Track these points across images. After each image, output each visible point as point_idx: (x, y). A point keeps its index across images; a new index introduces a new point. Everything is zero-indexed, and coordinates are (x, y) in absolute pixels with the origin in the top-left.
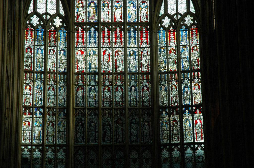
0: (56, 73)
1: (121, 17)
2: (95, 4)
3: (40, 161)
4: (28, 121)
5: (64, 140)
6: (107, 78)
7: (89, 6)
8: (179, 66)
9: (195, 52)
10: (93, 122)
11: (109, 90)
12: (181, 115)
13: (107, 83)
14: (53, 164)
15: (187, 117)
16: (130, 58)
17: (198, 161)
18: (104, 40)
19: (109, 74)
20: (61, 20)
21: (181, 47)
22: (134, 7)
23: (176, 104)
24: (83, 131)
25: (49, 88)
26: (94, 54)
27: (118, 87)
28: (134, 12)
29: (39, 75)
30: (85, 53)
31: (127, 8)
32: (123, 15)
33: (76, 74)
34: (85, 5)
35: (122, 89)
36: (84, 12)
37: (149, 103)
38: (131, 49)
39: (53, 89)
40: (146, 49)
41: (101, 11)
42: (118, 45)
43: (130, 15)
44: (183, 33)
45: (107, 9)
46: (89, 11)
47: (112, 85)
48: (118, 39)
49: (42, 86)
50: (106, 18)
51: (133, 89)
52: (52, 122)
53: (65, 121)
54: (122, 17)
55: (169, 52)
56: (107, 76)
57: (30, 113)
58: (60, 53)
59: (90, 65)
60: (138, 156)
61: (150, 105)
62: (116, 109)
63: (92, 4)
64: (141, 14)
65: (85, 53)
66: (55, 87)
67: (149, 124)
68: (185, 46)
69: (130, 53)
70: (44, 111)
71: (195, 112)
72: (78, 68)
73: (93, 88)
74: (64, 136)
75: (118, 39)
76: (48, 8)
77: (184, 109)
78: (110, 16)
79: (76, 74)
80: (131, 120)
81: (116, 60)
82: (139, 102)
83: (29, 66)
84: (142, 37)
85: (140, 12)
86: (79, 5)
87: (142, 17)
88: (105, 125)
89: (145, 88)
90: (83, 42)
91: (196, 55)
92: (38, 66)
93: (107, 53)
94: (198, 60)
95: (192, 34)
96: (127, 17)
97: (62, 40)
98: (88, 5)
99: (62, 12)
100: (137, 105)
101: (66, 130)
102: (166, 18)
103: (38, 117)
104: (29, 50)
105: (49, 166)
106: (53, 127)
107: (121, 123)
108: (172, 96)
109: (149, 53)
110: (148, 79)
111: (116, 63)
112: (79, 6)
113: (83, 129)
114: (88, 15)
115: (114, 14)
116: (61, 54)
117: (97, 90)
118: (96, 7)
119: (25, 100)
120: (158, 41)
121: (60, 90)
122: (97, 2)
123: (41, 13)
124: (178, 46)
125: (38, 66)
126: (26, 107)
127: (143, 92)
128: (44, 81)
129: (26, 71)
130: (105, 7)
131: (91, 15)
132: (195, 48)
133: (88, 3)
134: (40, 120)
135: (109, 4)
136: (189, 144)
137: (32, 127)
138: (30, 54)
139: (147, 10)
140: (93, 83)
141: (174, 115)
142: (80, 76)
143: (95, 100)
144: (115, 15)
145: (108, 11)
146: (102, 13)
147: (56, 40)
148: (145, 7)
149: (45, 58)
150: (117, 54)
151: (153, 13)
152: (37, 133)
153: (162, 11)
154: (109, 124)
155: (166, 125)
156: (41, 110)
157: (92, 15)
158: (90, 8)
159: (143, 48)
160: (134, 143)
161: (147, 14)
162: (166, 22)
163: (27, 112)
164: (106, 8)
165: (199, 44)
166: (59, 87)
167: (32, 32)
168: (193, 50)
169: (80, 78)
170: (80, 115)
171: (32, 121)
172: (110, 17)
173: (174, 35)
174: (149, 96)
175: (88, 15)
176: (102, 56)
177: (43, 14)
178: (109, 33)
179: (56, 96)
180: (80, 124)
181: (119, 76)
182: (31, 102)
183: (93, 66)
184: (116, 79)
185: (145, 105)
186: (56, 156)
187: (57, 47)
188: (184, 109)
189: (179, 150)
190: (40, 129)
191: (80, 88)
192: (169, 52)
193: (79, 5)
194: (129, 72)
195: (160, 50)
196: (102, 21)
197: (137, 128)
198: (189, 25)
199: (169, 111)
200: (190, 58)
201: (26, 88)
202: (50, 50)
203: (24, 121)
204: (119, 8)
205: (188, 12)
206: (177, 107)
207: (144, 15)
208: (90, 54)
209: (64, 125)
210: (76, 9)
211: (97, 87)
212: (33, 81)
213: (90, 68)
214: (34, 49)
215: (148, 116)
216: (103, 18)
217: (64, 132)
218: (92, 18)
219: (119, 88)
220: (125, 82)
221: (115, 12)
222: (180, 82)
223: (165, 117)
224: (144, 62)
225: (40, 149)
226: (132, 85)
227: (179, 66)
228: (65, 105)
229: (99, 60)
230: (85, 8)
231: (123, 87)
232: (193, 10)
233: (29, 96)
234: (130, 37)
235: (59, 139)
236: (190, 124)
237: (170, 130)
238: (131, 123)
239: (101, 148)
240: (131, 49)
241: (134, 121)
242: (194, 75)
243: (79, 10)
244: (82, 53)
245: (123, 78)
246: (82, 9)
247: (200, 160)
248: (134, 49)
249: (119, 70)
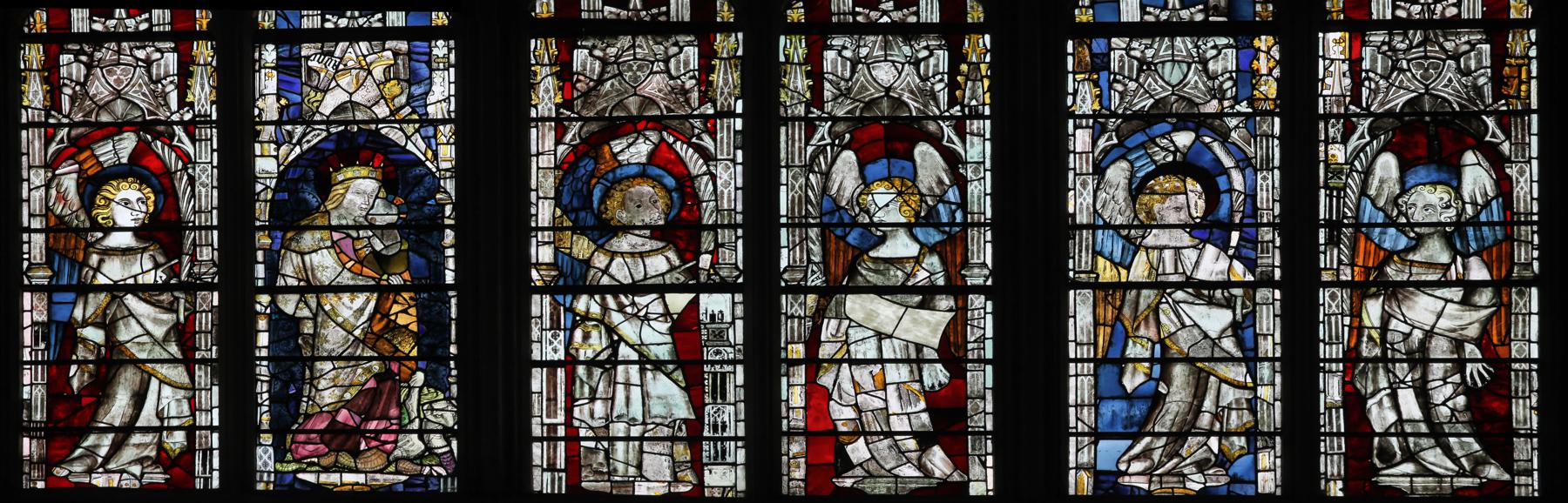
22: (1209, 229)
28: (1216, 320)
31: (1081, 259)
32: (981, 379)
34: (208, 195)
36: (183, 334)
41: (540, 306)
43: (1133, 380)
46: (289, 304)
54: (962, 415)
64: (1366, 350)
78: (720, 392)
85: (1358, 329)
86: (88, 202)
87: (1380, 416)
96: (1079, 418)
98: (262, 212)
112: (101, 214)
114: (263, 370)
115: (798, 351)
130: (604, 231)
135: (705, 188)
139: (1500, 285)
144: (826, 380)
145: (678, 302)
146: (548, 347)
148: (1455, 234)
157: (344, 377)
161: (1500, 365)
172: (730, 415)
175: (263, 370)
193: (88, 202)
204: (913, 249)
207: (1437, 370)
210: (41, 277)
216: (572, 438)
221: (829, 328)
243: (97, 301)
246: (161, 276)
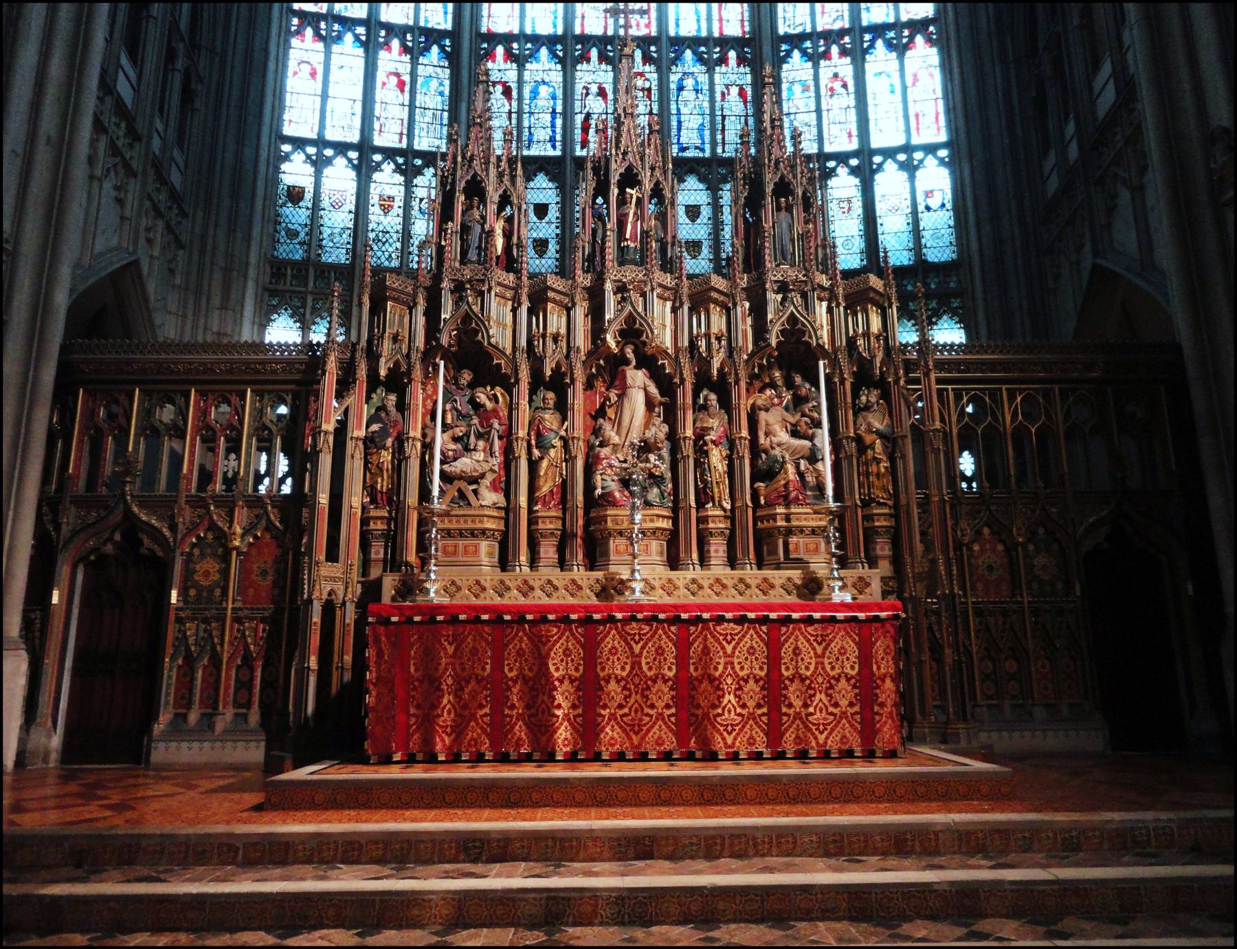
3: (348, 201)
4: (308, 63)
5: (441, 138)
12: (858, 55)
14: (398, 215)
17: (928, 208)
24: (510, 113)
37: (743, 26)
53: (447, 77)
57: (318, 36)
60: (704, 198)
61: (744, 33)
67: (742, 93)
74: (441, 124)
77: (867, 37)
80: (681, 80)
88: (587, 94)
100: (699, 29)
101: (450, 105)
105: (382, 218)
106: (402, 91)
107: (643, 90)
113: (510, 105)
136: (889, 153)
141: (830, 59)
155: (807, 94)
156: (361, 30)
160: (688, 154)
186: (409, 186)
188: (867, 37)
189: (854, 171)
199: (816, 46)
206: (842, 33)
209: (442, 88)
215: (739, 65)
217: (443, 110)
223: (796, 68)
225: (350, 161)
228: (448, 26)
235: (423, 134)
237: (818, 111)
239: (573, 166)
247: (934, 203)
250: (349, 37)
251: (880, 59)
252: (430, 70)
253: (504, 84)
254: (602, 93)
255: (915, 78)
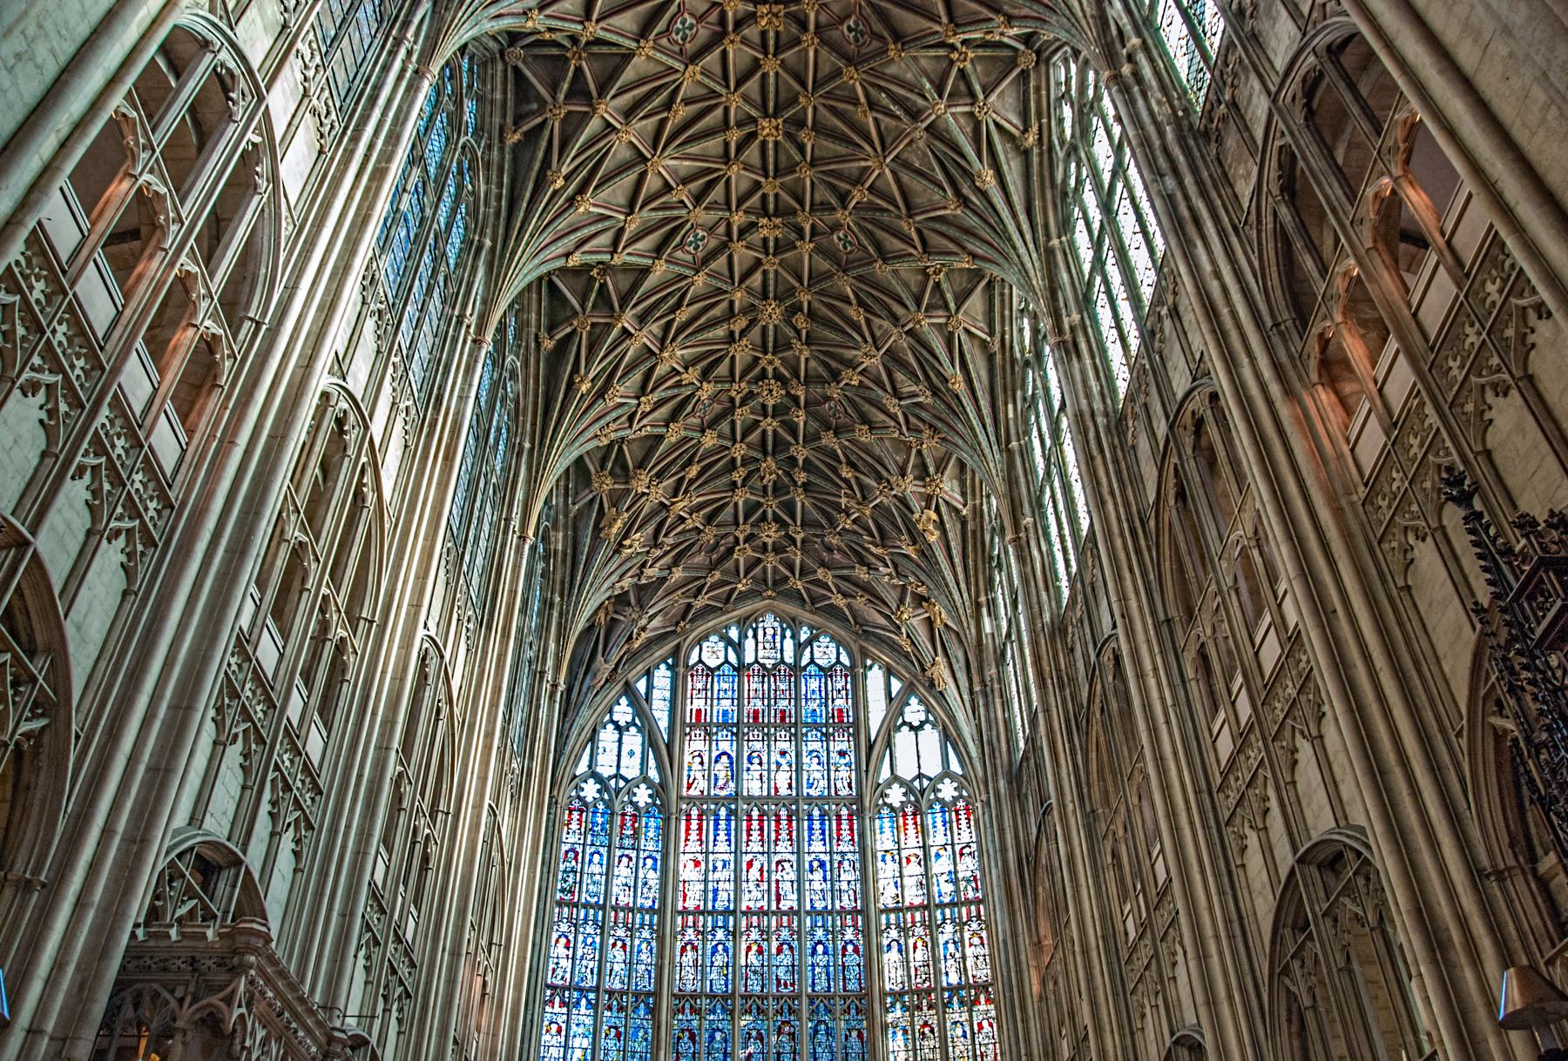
0: (632, 910)
1: (790, 785)
2: (729, 757)
6: (755, 924)
7: (716, 762)
8: (929, 895)
9: (968, 860)
10: (719, 1030)
11: (760, 951)
13: (755, 935)
15: (957, 1014)
16: (811, 877)
18: (749, 835)
19: (761, 912)
20: (650, 792)
21: (933, 851)
23: (927, 984)
24: (694, 1053)
25: (614, 945)
26: (724, 866)
27: (782, 945)
29: (592, 912)
30: (703, 864)
33: (681, 913)
35: (791, 948)
38: (813, 856)
39: (624, 947)
40: (849, 856)
42: (784, 846)
44: (935, 819)
45: (759, 767)
47: (767, 940)
48: (784, 835)
49: (598, 939)
50: (753, 786)
51: (820, 948)
52: (616, 1028)
55: (904, 861)
56: (755, 918)
57: (563, 1004)
58: (645, 864)
59: (716, 891)
61: (861, 989)
62: (777, 998)
63: (724, 759)
65: (703, 864)
66: (629, 943)
67: (860, 1035)
68: (944, 847)
69: (811, 866)
70: (597, 999)
71: (976, 1002)
72: (684, 900)
73: (720, 947)
75: (784, 835)
76: (622, 764)
79: (681, 913)
80: (816, 1025)
81: (777, 881)
82: (834, 980)
83: (570, 891)
84: (839, 829)
89: (850, 948)
90: (700, 840)
91: (968, 866)
92: (590, 891)
93: (757, 865)
94: (975, 877)
95: (958, 820)
97: (651, 834)
99: (653, 774)
100: (829, 987)
102: (896, 786)
103: (583, 1014)
104: (571, 855)
107: (789, 1034)
108: (917, 964)
109: (857, 865)
110: (855, 926)
111: (777, 888)
116: (648, 866)
117: (731, 952)
118: (731, 763)
119: (554, 970)
120: (878, 837)
121: (640, 951)
122: (734, 755)
123: (606, 775)
124: (925, 847)
125: (590, 891)
126: (553, 987)
127: (844, 955)
128: (602, 928)
129: (560, 903)
131: (720, 783)
132: (967, 851)
133: (715, 754)
134: (587, 1022)
137: (567, 1037)
138: (574, 863)
140: (720, 935)
142: (691, 918)
143: (726, 975)
147: (636, 835)
149: (608, 874)
150: (780, 868)
151: (864, 775)
152: (578, 1054)
153: (885, 773)
154: (759, 1034)
156: (592, 996)
158: (719, 766)
159: (843, 854)
162: (896, 796)
163: (557, 1000)
164: (756, 767)
165: (974, 839)
166: (637, 942)
167: (581, 815)
168: (962, 854)
169: (690, 924)
170: (687, 1011)
171: (568, 1022)
172: (765, 786)
173: (915, 823)
174: (859, 965)
176: (744, 873)
177: (610, 778)
178: (761, 821)
179: (630, 965)
180: (687, 1033)
181: (785, 918)
182: (568, 976)
183: (723, 896)
184: (780, 925)
185: (849, 988)
187: (638, 850)
190: (586, 1043)
191: (689, 947)
192: (904, 861)
194: (808, 907)
195: (884, 856)
196: (745, 794)
197: (831, 1046)
198: (948, 799)
200: (956, 872)
201: (557, 941)
202: (621, 857)
203: (546, 1023)
205: (947, 773)
206: (928, 992)
208: (715, 868)
211: (730, 945)
212: (575, 925)
213: (715, 900)
214: (583, 852)
218: (721, 788)
219: (785, 947)
220: (799, 932)
222: (932, 928)
224: (844, 886)
226: (817, 938)
227: (929, 895)
229: (737, 880)
230: (706, 766)
231: (795, 944)
232: (955, 767)
233: (563, 963)
234: (811, 829)
236: (964, 1032)
238: (816, 1032)
240: (813, 856)
241: (823, 1026)
242: (969, 912)
244: (697, 864)
245: (795, 924)
248: (823, 857)
249: (784, 906)
250: (584, 1002)
251: (957, 1014)
252: (639, 1022)
253: (690, 1031)
254: (760, 1037)
255: (980, 1026)
